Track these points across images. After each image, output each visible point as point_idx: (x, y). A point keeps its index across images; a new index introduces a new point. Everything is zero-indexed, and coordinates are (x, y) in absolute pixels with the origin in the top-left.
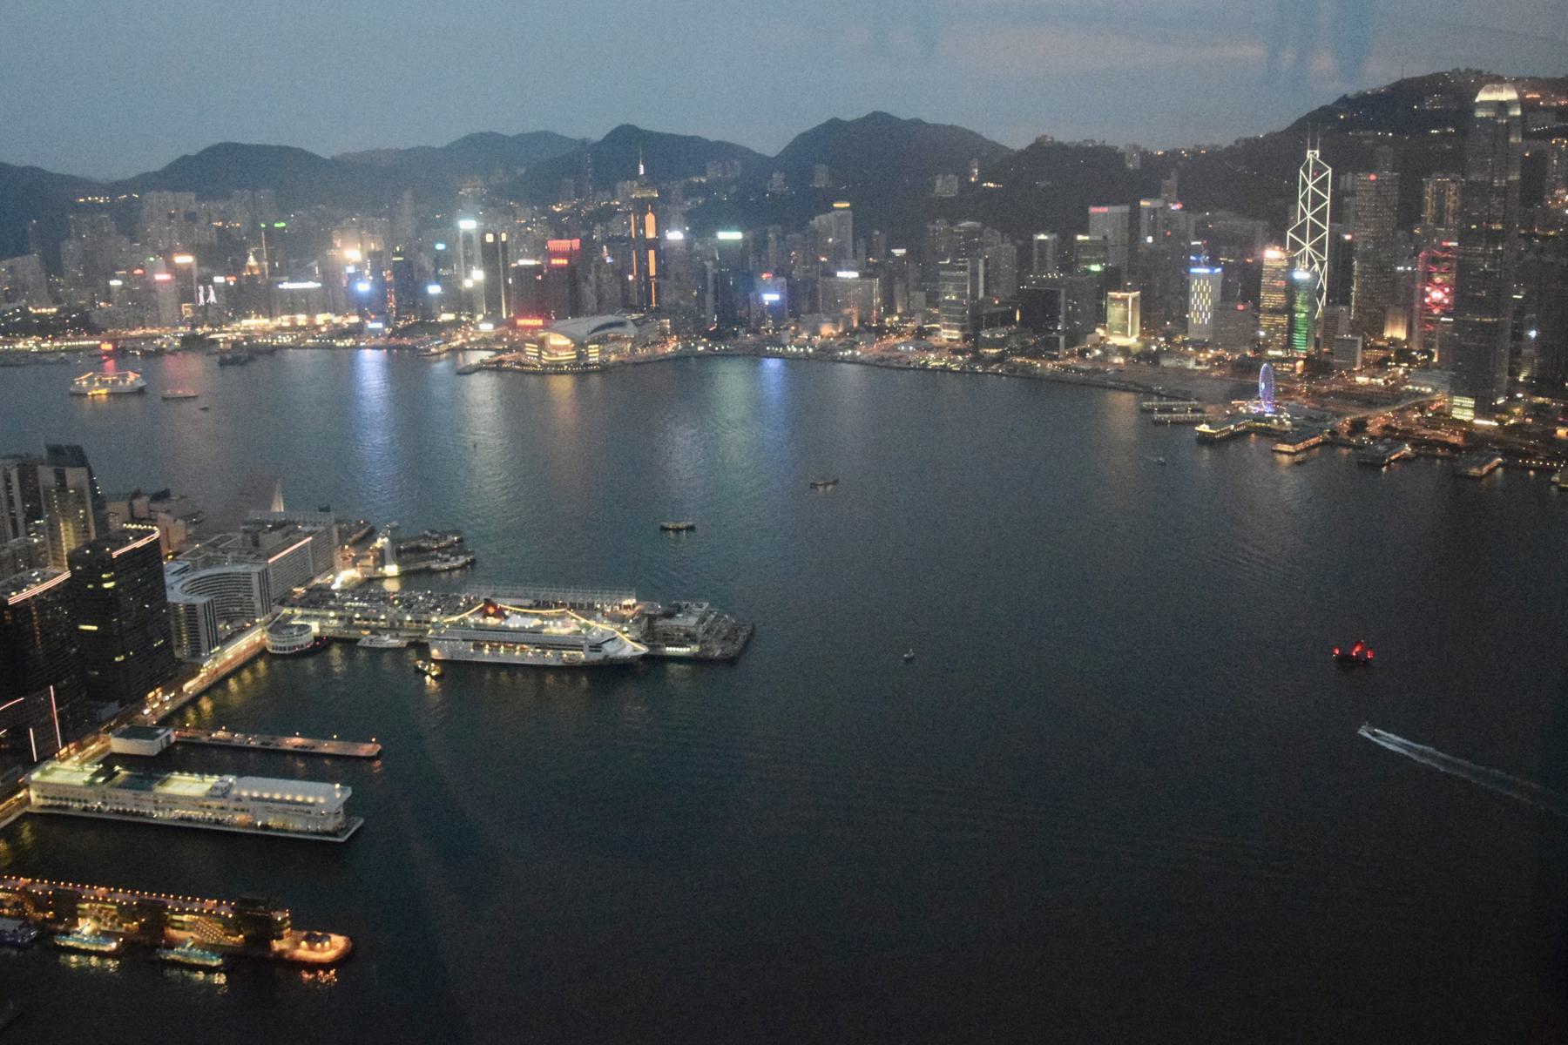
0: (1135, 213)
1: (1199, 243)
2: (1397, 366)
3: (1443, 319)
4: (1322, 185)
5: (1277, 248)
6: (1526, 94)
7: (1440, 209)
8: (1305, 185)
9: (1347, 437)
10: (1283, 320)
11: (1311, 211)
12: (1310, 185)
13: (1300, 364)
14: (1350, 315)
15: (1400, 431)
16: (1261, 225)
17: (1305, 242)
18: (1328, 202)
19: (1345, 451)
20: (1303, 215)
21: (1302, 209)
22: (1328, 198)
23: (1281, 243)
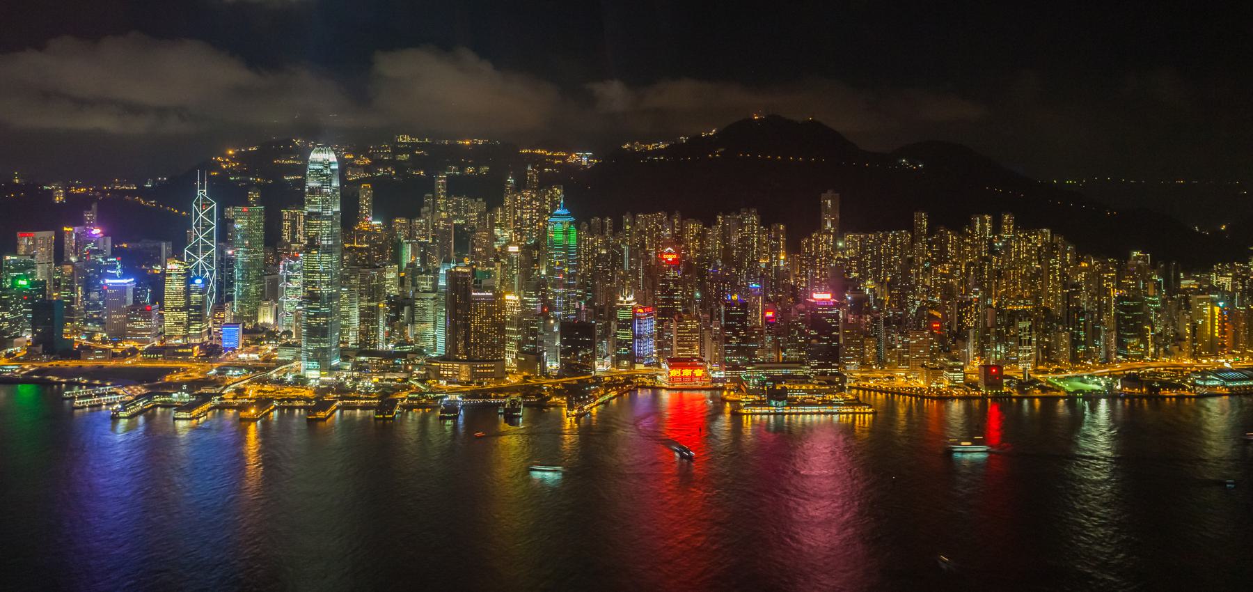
1: (115, 259)
2: (268, 343)
3: (297, 308)
5: (176, 261)
6: (345, 155)
7: (294, 233)
8: (197, 214)
9: (232, 401)
10: (184, 315)
12: (201, 215)
16: (165, 247)
19: (231, 412)
20: (197, 237)
21: (195, 232)
22: (215, 224)
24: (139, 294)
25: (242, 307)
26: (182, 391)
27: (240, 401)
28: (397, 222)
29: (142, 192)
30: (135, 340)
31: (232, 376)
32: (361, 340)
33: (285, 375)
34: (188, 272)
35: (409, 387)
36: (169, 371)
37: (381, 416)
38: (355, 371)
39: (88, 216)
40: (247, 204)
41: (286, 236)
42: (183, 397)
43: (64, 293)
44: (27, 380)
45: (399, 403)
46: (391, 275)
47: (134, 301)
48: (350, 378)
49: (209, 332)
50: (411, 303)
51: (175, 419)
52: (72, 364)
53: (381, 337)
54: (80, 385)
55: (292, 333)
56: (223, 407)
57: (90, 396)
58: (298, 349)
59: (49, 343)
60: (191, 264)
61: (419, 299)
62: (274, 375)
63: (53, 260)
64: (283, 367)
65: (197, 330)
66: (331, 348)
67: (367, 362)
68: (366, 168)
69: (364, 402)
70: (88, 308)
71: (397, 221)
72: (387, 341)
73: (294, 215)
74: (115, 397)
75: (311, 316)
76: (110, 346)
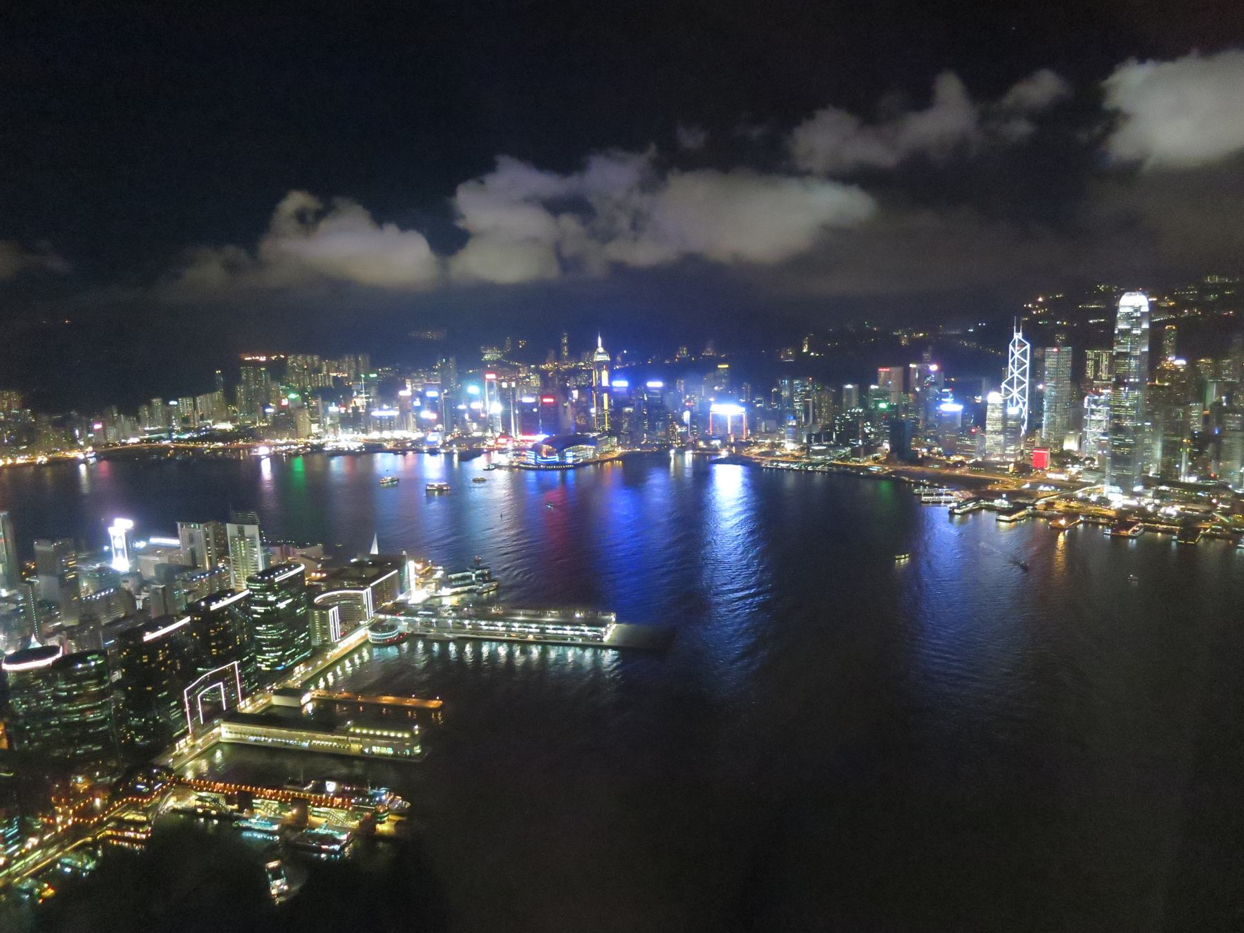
0: (907, 371)
2: (1072, 467)
4: (1024, 354)
8: (1013, 354)
10: (1001, 438)
11: (1018, 369)
12: (1017, 355)
13: (1012, 466)
14: (1042, 435)
15: (1076, 508)
16: (984, 382)
17: (1013, 389)
18: (1027, 366)
19: (1042, 520)
20: (1012, 373)
23: (999, 391)
24: (966, 418)
25: (1049, 434)
26: (1002, 499)
27: (1050, 513)
28: (1203, 362)
29: (967, 336)
30: (962, 455)
31: (1042, 491)
32: (1162, 472)
33: (1089, 495)
34: (1005, 404)
35: (1213, 518)
36: (992, 482)
37: (1183, 542)
38: (1157, 498)
39: (926, 355)
40: (1053, 345)
41: (1090, 373)
42: (1001, 503)
43: (912, 415)
44: (887, 477)
45: (1202, 532)
46: (1196, 412)
47: (962, 424)
48: (1150, 504)
49: (1022, 452)
50: (1217, 440)
51: (997, 520)
52: (917, 469)
53: (1183, 470)
54: (925, 486)
55: (1094, 460)
56: (1035, 515)
57: (932, 495)
58: (1099, 474)
59: (901, 452)
60: (1008, 395)
61: (1226, 437)
62: (1079, 494)
63: (901, 389)
64: (1087, 488)
65: (1011, 450)
66: (1133, 476)
67: (1168, 491)
68: (1170, 310)
69: (1165, 526)
70: (927, 427)
71: (1202, 360)
72: (1190, 474)
73: (1097, 355)
74: (953, 497)
75: (1116, 446)
76: (944, 458)
